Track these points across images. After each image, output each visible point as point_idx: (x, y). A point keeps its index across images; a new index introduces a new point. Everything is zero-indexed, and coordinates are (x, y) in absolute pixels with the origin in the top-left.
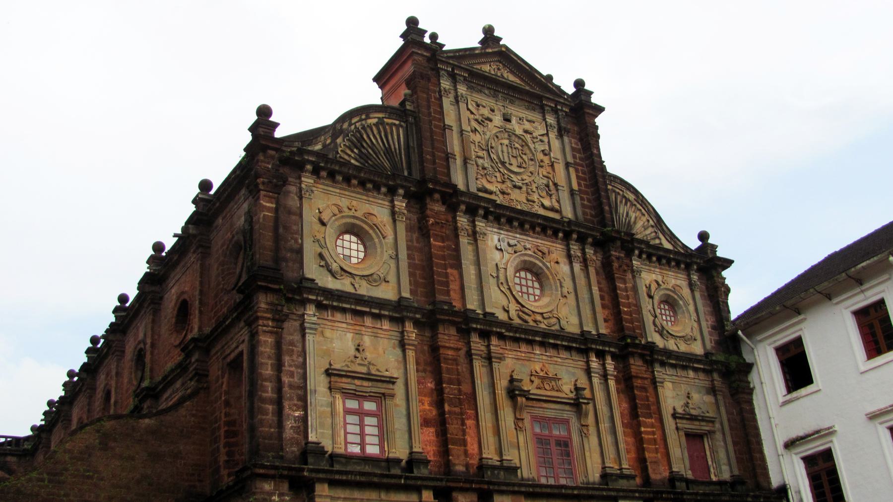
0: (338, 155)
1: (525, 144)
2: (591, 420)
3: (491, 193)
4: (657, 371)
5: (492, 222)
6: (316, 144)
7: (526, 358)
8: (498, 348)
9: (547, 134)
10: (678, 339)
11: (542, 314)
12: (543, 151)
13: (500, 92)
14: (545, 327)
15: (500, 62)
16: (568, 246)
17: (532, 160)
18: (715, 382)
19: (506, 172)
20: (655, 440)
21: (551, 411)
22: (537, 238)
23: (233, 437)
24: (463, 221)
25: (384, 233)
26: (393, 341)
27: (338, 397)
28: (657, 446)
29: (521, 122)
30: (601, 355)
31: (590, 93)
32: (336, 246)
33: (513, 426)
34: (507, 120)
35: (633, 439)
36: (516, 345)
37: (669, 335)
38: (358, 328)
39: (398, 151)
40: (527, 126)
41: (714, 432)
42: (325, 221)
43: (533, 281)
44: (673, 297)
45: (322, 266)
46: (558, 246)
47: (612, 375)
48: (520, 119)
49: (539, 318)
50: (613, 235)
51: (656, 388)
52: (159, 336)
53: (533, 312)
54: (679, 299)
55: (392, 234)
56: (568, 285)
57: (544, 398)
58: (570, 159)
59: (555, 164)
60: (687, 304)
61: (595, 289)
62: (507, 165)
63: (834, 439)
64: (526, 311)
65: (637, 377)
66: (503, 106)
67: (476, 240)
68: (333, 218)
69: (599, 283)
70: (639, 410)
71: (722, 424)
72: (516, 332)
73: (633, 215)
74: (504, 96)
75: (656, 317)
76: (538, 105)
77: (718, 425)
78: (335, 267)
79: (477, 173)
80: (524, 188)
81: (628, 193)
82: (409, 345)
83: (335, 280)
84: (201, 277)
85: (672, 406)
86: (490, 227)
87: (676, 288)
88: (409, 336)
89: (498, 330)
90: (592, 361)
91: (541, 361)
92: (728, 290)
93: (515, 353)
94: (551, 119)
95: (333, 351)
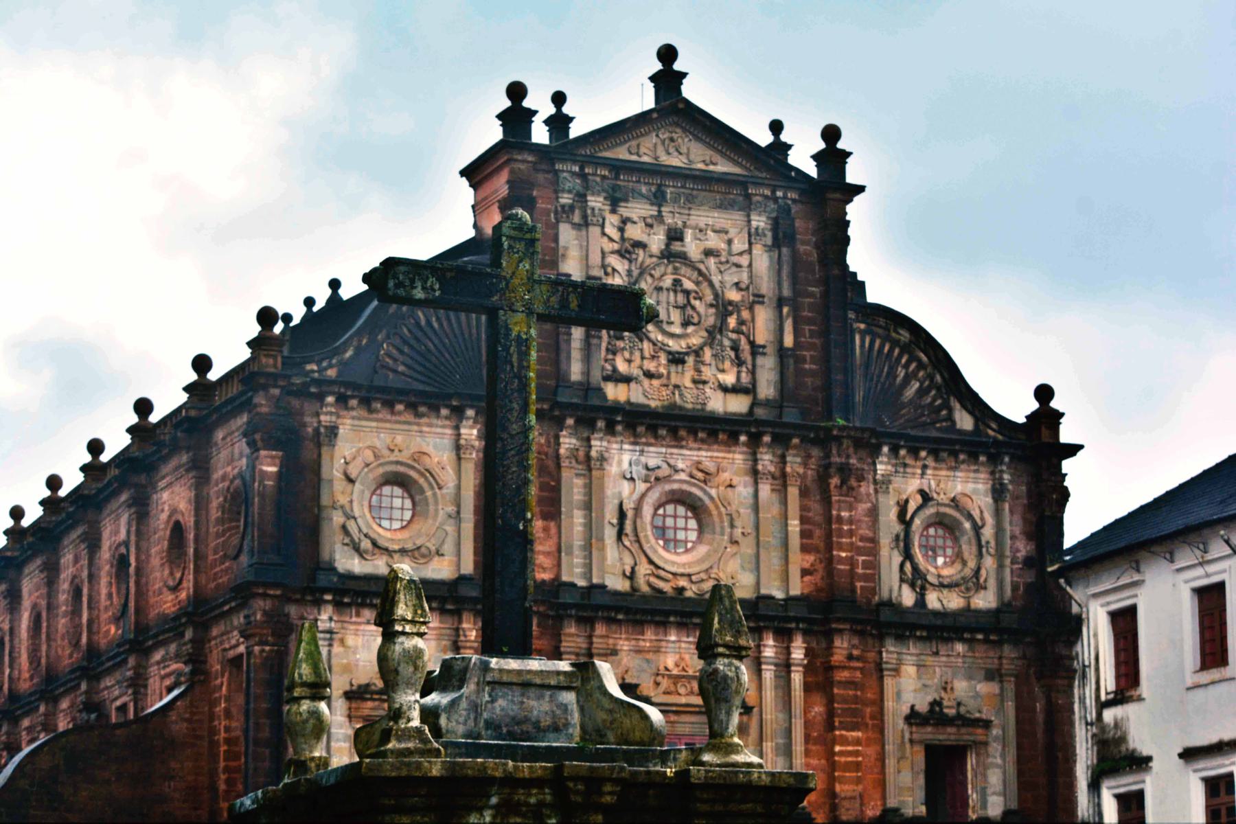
0: (378, 364)
1: (704, 277)
3: (627, 380)
4: (887, 651)
5: (621, 434)
6: (346, 351)
9: (750, 251)
10: (945, 591)
11: (689, 575)
12: (737, 284)
13: (669, 186)
15: (677, 125)
16: (754, 454)
17: (711, 305)
18: (1005, 661)
19: (660, 338)
20: (858, 764)
22: (699, 449)
24: (568, 442)
25: (440, 482)
26: (444, 642)
28: (859, 774)
29: (699, 236)
30: (785, 636)
34: (675, 236)
35: (823, 761)
37: (927, 586)
40: (714, 241)
41: (986, 744)
42: (353, 476)
43: (686, 518)
44: (951, 516)
48: (701, 231)
49: (683, 583)
50: (835, 432)
51: (881, 678)
52: (148, 556)
53: (674, 574)
54: (962, 519)
57: (674, 708)
58: (786, 292)
60: (977, 529)
61: (794, 525)
62: (665, 326)
63: (1149, 779)
64: (662, 573)
65: (844, 668)
66: (671, 212)
67: (590, 470)
68: (366, 470)
69: (803, 508)
73: (901, 373)
75: (908, 555)
76: (741, 195)
77: (995, 731)
78: (366, 544)
79: (607, 350)
80: (690, 360)
81: (901, 332)
82: (465, 648)
83: (363, 562)
84: (197, 515)
85: (909, 705)
86: (617, 442)
88: (465, 636)
89: (606, 614)
90: (765, 646)
92: (1065, 495)
93: (633, 643)
94: (760, 221)
95: (357, 666)
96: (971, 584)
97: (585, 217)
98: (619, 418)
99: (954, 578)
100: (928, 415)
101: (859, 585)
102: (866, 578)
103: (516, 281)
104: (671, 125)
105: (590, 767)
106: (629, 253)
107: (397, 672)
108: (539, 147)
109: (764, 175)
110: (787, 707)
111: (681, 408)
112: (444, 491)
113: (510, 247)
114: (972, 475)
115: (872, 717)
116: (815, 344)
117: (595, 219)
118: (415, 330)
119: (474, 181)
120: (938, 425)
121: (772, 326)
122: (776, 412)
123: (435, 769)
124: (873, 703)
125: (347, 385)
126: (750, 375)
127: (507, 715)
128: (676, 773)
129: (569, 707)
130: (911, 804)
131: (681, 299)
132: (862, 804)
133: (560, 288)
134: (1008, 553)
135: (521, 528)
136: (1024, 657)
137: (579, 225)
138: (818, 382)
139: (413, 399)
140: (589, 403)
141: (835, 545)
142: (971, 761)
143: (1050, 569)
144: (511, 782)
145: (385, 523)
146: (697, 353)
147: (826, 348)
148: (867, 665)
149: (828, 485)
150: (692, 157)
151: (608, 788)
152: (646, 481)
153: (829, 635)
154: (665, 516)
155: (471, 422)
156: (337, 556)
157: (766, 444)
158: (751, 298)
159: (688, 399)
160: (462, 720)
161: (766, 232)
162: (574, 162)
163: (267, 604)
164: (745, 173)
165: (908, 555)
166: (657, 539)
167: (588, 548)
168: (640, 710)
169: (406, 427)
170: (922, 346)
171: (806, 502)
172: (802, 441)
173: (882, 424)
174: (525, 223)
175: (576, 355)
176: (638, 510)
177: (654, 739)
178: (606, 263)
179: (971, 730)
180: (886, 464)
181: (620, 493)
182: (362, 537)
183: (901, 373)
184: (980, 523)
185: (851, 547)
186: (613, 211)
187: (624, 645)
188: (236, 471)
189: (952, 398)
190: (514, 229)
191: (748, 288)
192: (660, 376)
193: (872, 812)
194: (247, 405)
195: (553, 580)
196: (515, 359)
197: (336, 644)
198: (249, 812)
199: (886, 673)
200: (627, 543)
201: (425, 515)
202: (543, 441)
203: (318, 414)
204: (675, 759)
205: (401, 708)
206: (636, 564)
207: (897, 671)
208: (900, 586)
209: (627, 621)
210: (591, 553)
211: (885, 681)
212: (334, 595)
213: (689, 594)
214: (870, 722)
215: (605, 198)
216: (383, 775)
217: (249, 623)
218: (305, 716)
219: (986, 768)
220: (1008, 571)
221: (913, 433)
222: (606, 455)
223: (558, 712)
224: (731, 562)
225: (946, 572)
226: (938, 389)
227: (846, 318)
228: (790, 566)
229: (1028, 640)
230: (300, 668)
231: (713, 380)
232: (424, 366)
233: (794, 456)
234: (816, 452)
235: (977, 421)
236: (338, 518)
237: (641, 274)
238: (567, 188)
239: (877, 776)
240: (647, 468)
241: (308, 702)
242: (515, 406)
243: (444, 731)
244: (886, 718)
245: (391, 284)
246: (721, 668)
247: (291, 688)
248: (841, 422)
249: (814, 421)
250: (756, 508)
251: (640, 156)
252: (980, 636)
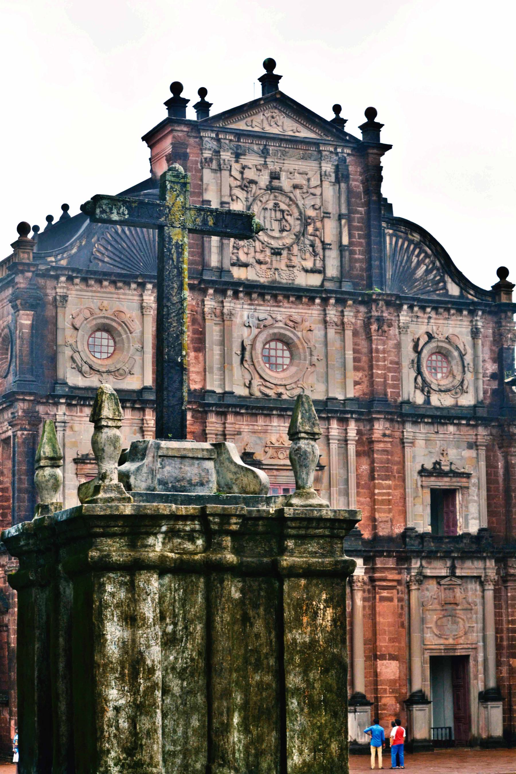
0: (93, 257)
8: (234, 426)
9: (321, 186)
10: (443, 394)
11: (285, 385)
12: (313, 206)
14: (287, 398)
15: (276, 108)
16: (325, 310)
17: (298, 219)
18: (479, 437)
19: (266, 239)
20: (389, 501)
22: (291, 308)
23: (6, 502)
24: (210, 303)
25: (131, 329)
26: (134, 428)
29: (290, 176)
30: (343, 421)
31: (380, 126)
34: (275, 176)
35: (368, 499)
36: (254, 419)
37: (432, 391)
39: (152, 239)
40: (299, 180)
41: (468, 488)
42: (77, 326)
43: (283, 350)
44: (446, 348)
45: (74, 368)
46: (314, 312)
48: (291, 173)
49: (281, 390)
50: (374, 297)
51: (404, 447)
55: (140, 327)
56: (319, 351)
57: (276, 467)
58: (344, 211)
59: (326, 220)
60: (462, 356)
61: (350, 354)
62: (269, 232)
64: (268, 384)
67: (223, 321)
68: (85, 322)
69: (355, 344)
70: (376, 473)
71: (479, 479)
72: (252, 409)
73: (415, 260)
74: (276, 148)
75: (419, 372)
77: (474, 480)
78: (86, 368)
79: (234, 247)
80: (285, 253)
81: (414, 235)
82: (148, 431)
83: (85, 379)
85: (421, 464)
87: (454, 339)
88: (147, 424)
89: (234, 410)
93: (251, 427)
94: (328, 167)
95: (81, 443)
96: (458, 390)
97: (219, 165)
98: (241, 289)
99: (448, 386)
100: (432, 286)
101: (389, 390)
102: (394, 386)
103: (175, 209)
104: (272, 108)
105: (223, 508)
106: (247, 187)
107: (103, 450)
108: (189, 123)
109: (329, 138)
110: (346, 466)
111: (279, 283)
112: (134, 334)
113: (171, 188)
114: (459, 323)
116: (361, 243)
117: (225, 166)
118: (114, 235)
119: (150, 144)
120: (438, 292)
121: (335, 232)
122: (338, 284)
123: (128, 510)
124: (398, 463)
125: (73, 270)
126: (322, 262)
127: (172, 476)
128: (276, 511)
129: (210, 471)
130: (422, 525)
131: (279, 215)
132: (392, 525)
133: (202, 213)
134: (481, 371)
135: (179, 361)
136: (491, 434)
137: (216, 170)
138: (364, 267)
139: (114, 278)
140: (223, 280)
141: (374, 367)
142: (459, 498)
143: (507, 381)
144: (174, 517)
145: (98, 355)
146: (289, 249)
147: (369, 244)
148: (395, 440)
149: (370, 329)
150: (285, 128)
151: (234, 520)
152: (258, 328)
153: (371, 421)
154: (270, 349)
155: (150, 292)
156: (68, 375)
157: (332, 304)
158: (322, 214)
159: (284, 278)
160: (144, 479)
161: (331, 174)
162: (212, 131)
163: (26, 406)
164: (318, 138)
165: (419, 372)
166: (265, 363)
167: (223, 369)
168: (253, 472)
169: (109, 295)
170: (428, 243)
171: (356, 340)
172: (354, 302)
173: (403, 292)
174: (180, 173)
175: (214, 250)
176: (253, 346)
177: (262, 490)
178: (233, 193)
179: (458, 479)
180: (407, 316)
181: (242, 335)
182: (84, 364)
183: (415, 260)
184: (463, 352)
185: (385, 368)
186: (237, 161)
187: (245, 429)
188: (5, 323)
189: (446, 276)
190: (174, 176)
191: (320, 208)
192: (266, 263)
193: (398, 530)
194: (11, 283)
195: (202, 389)
196: (175, 257)
197: (68, 429)
198: (13, 537)
199: (406, 445)
200: (246, 366)
201: (122, 350)
202: (194, 304)
203: (55, 288)
204: (275, 502)
205: (105, 473)
206: (252, 379)
208: (415, 391)
209: (247, 414)
210: (224, 372)
211: (406, 450)
212: (66, 399)
213: (284, 397)
214: (397, 475)
215: (232, 153)
216: (95, 513)
217: (14, 417)
218: (47, 478)
219: (468, 502)
220: (481, 382)
221: (422, 297)
222: (233, 312)
223: (203, 474)
224: (310, 378)
225: (442, 383)
226: (438, 270)
227: (380, 226)
228: (347, 379)
229: (493, 424)
230: (44, 448)
231: (299, 265)
232: (120, 258)
233: (350, 311)
234: (362, 309)
235: (462, 289)
236: (68, 352)
237: (254, 200)
238: (208, 147)
239: (401, 508)
240: (259, 320)
241: (49, 468)
242: (175, 286)
243: (133, 486)
245: (98, 211)
246: (303, 446)
247: (39, 460)
248: (379, 291)
249: (362, 290)
251: (253, 127)
252: (464, 422)
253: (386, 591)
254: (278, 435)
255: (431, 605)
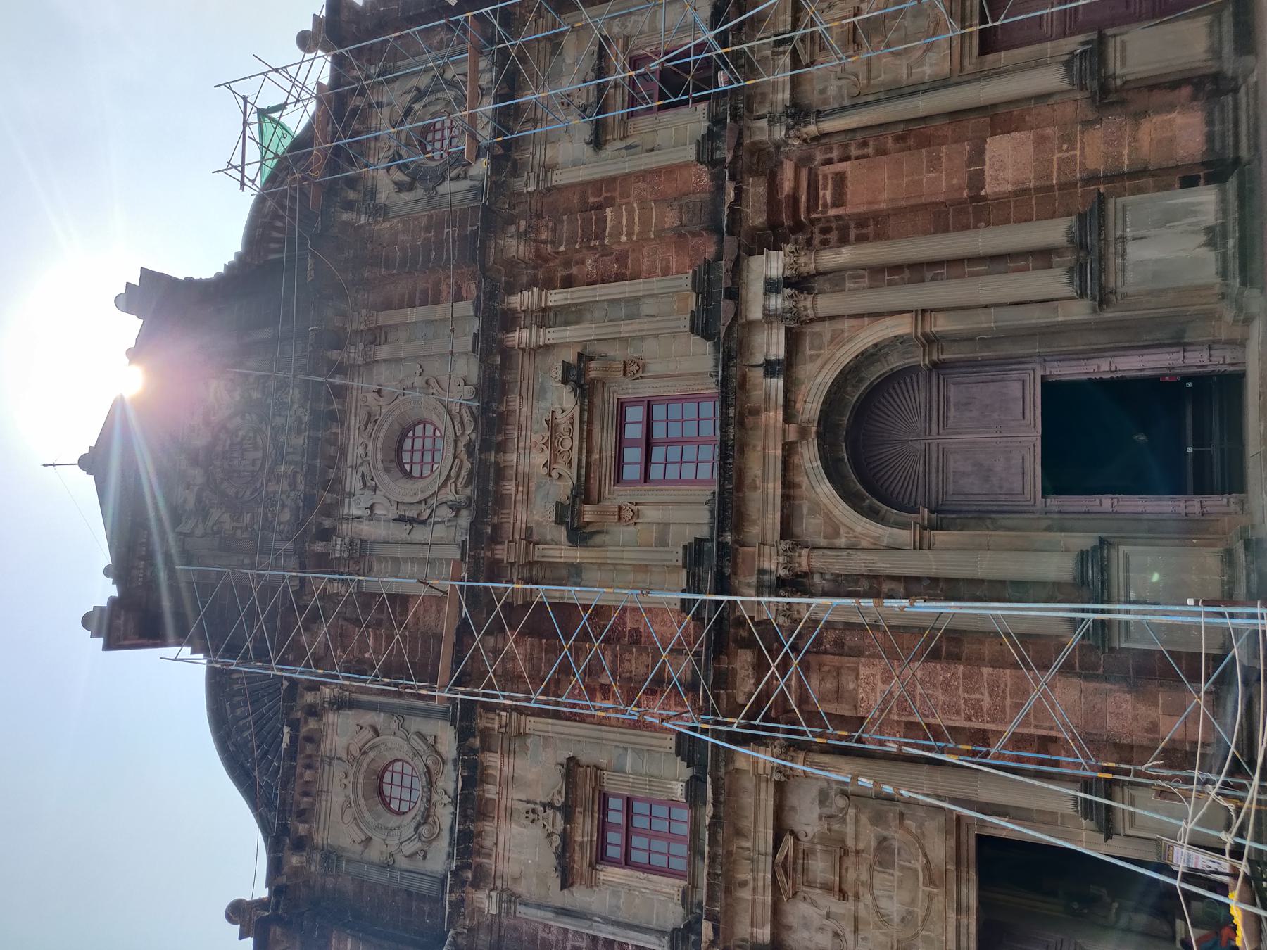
2: (616, 352)
7: (526, 479)
21: (605, 438)
22: (349, 429)
26: (517, 748)
27: (601, 876)
30: (510, 320)
32: (399, 813)
33: (632, 528)
38: (502, 813)
41: (627, 39)
43: (414, 438)
47: (540, 297)
57: (584, 456)
61: (413, 314)
80: (283, 439)
91: (528, 451)
112: (380, 727)
115: (598, 192)
178: (209, 531)
184: (414, 93)
187: (522, 517)
207: (550, 168)
211: (559, 183)
213: (473, 436)
214: (604, 195)
244: (597, 176)
250: (399, 361)
253: (821, 193)
254: (534, 450)
255: (857, 76)
